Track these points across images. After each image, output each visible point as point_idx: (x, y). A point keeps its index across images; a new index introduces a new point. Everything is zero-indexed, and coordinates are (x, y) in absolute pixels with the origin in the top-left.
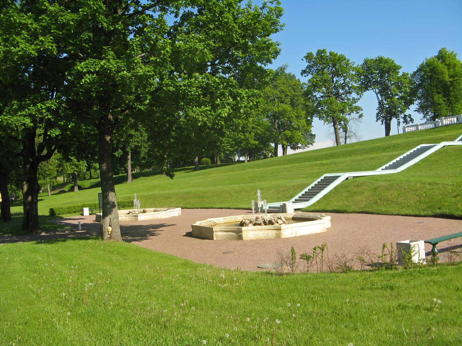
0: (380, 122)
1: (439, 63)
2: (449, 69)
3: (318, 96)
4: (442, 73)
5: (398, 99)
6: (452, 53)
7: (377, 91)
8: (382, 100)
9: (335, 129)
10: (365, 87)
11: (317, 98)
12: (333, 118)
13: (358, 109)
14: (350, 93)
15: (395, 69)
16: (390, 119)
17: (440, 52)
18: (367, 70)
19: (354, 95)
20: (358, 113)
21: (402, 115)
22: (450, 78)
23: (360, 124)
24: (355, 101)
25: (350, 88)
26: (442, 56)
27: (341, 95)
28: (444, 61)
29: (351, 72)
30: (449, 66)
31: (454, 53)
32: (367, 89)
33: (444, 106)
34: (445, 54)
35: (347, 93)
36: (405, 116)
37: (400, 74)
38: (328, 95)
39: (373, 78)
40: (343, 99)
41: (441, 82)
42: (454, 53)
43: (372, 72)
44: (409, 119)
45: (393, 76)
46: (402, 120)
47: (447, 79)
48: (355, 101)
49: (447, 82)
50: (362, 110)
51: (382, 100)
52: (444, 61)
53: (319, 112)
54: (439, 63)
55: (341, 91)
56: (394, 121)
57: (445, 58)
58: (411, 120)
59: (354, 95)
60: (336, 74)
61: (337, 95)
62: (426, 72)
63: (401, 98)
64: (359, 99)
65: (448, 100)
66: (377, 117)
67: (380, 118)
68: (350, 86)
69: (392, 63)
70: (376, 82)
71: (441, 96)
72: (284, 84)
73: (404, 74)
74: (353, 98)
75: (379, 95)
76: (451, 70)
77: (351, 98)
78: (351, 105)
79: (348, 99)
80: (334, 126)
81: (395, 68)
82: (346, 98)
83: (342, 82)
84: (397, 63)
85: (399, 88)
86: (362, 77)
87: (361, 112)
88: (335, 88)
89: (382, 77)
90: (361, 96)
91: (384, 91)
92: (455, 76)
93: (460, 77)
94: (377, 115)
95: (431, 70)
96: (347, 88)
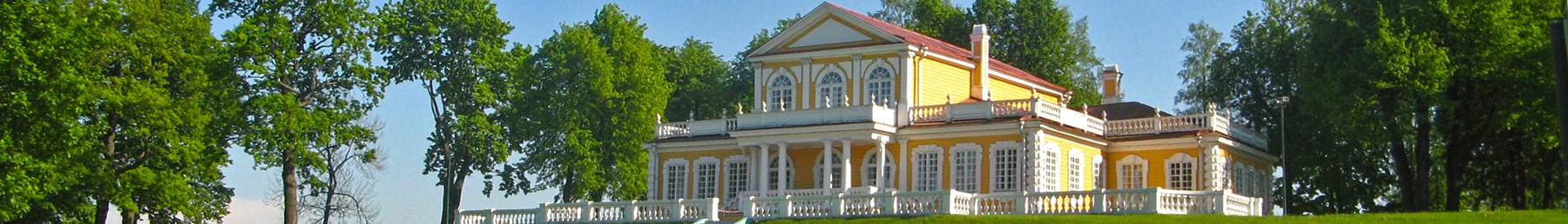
0: (434, 176)
1: (593, 45)
2: (616, 64)
3: (251, 82)
4: (597, 73)
5: (491, 119)
6: (631, 24)
7: (436, 85)
8: (447, 115)
9: (287, 186)
10: (402, 69)
11: (246, 86)
12: (285, 155)
13: (364, 135)
14: (349, 86)
15: (494, 33)
16: (464, 172)
17: (603, 16)
18: (411, 20)
19: (357, 94)
20: (361, 147)
21: (501, 167)
22: (617, 89)
23: (378, 174)
24: (357, 109)
25: (348, 72)
26: (605, 26)
27: (319, 89)
28: (606, 43)
29: (357, 26)
30: (618, 56)
31: (639, 23)
32: (407, 75)
33: (593, 165)
34: (615, 23)
35: (339, 84)
36: (508, 169)
37: (509, 48)
38: (279, 81)
39: (429, 46)
40: (323, 101)
41: (594, 95)
42: (639, 23)
43: (426, 28)
44: (517, 181)
45: (483, 50)
46: (497, 181)
47: (609, 92)
48: (357, 109)
49: (606, 100)
50: (374, 140)
51: (447, 115)
52: (609, 43)
53: (244, 127)
54: (593, 45)
55: (321, 76)
56: (473, 182)
57: (613, 34)
58: (521, 185)
59: (357, 94)
60: (314, 24)
61: (308, 88)
62: (557, 63)
63: (502, 116)
64: (370, 107)
65: (607, 146)
66: (427, 161)
67: (435, 164)
68: (349, 64)
69: (488, 12)
70: (438, 57)
71: (588, 133)
72: (156, 21)
73: (517, 51)
74: (355, 103)
75: (438, 99)
76: (623, 69)
77: (348, 99)
78: (344, 122)
79: (339, 104)
80: (285, 175)
81: (494, 31)
82: (333, 98)
83: (328, 51)
84: (502, 16)
85: (497, 86)
86: (397, 39)
87: (370, 146)
88: (309, 65)
89: (454, 46)
90: (375, 101)
91: (456, 90)
92: (633, 87)
93: (643, 90)
94: (430, 154)
95: (572, 62)
96: (339, 70)
